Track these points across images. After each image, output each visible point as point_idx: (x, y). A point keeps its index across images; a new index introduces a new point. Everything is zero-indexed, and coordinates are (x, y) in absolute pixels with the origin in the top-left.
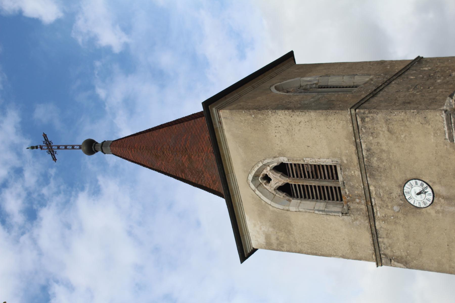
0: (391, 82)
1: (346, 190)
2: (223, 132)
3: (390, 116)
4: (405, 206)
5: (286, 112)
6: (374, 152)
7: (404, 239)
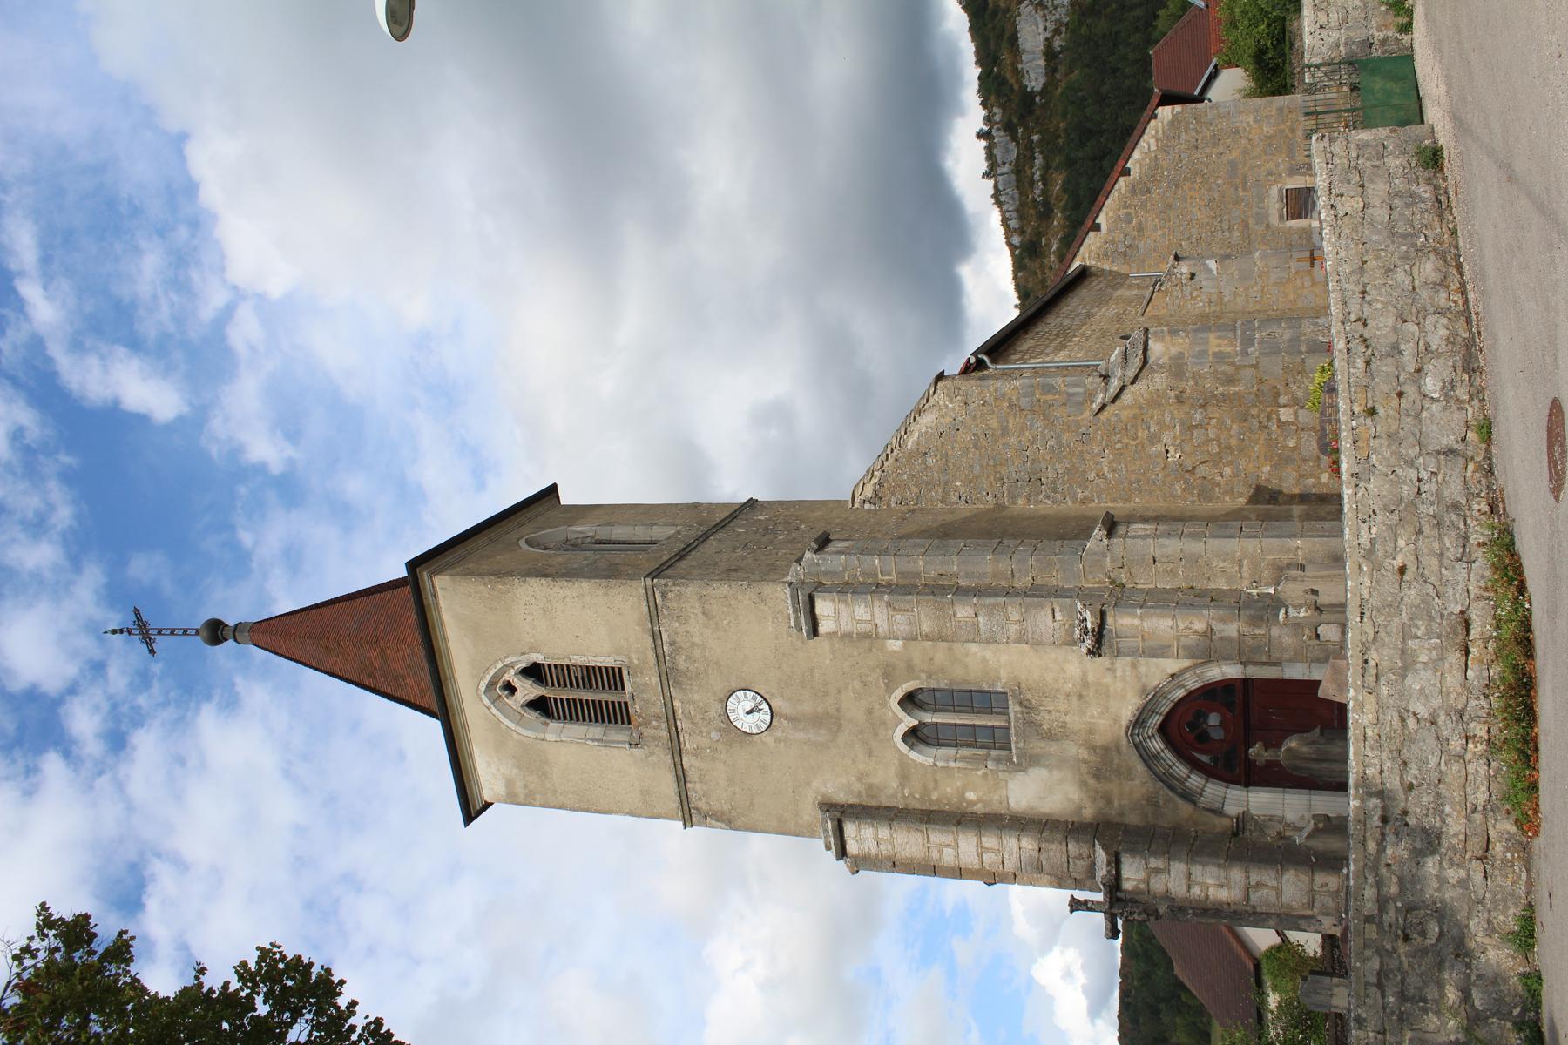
0: (708, 538)
1: (637, 707)
3: (706, 590)
5: (543, 581)
6: (681, 647)
7: (726, 784)
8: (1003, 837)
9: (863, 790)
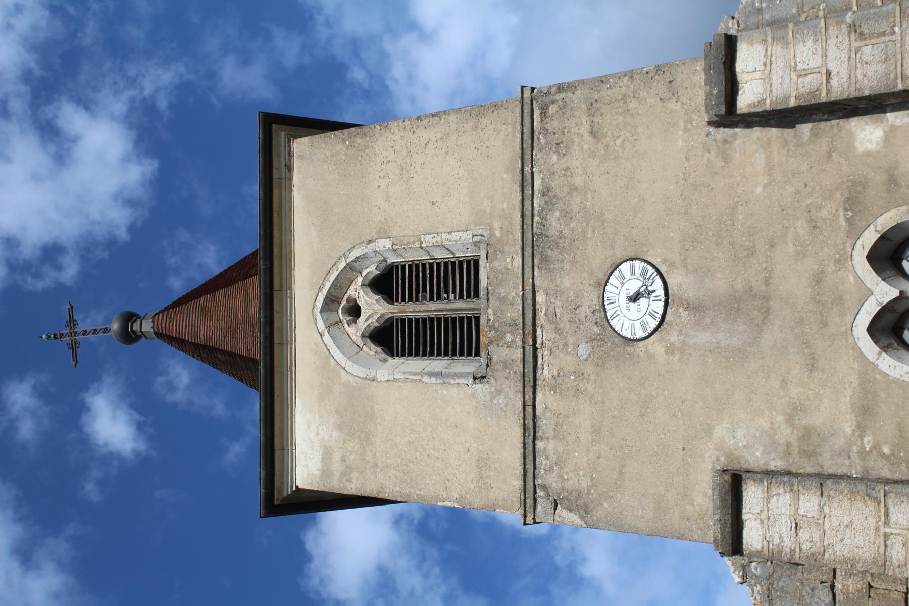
2: (290, 191)
4: (602, 340)
6: (555, 197)
9: (793, 440)
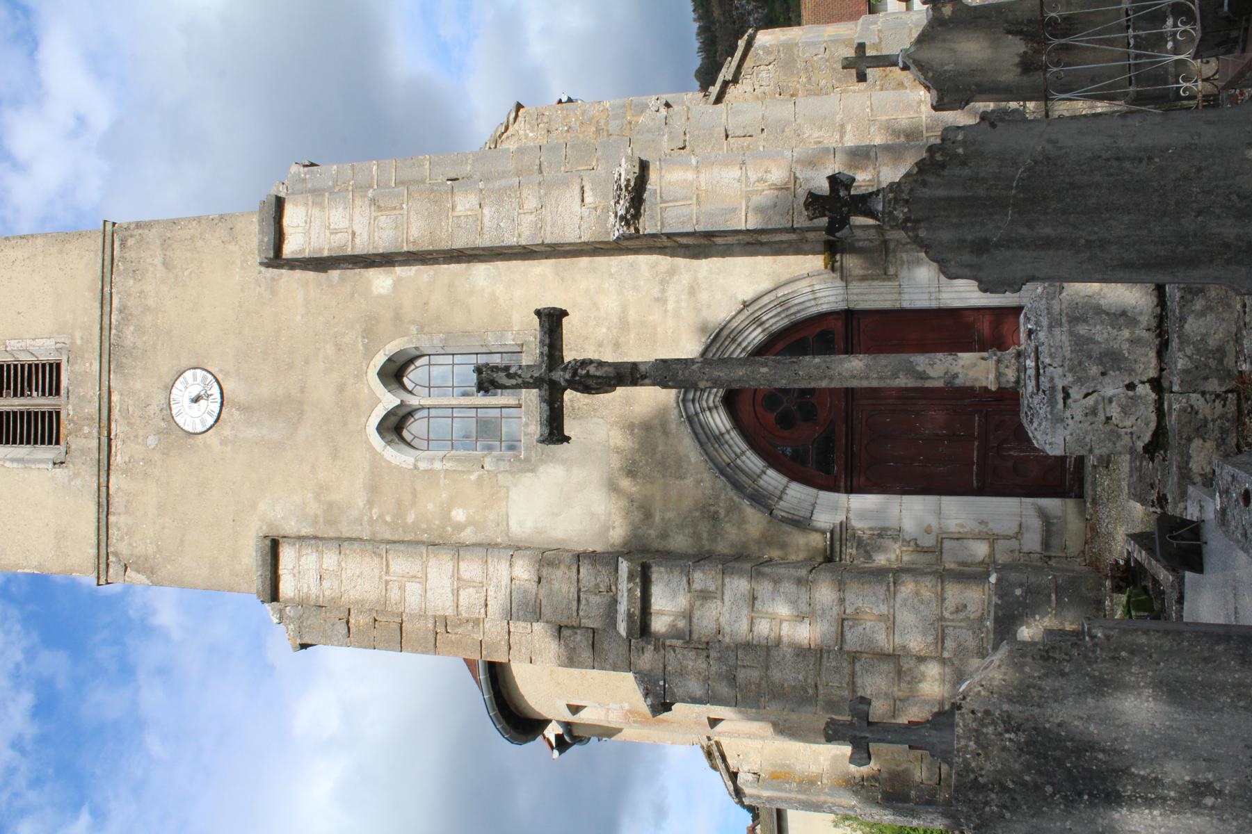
3: (171, 231)
4: (167, 433)
6: (131, 314)
8: (489, 561)
